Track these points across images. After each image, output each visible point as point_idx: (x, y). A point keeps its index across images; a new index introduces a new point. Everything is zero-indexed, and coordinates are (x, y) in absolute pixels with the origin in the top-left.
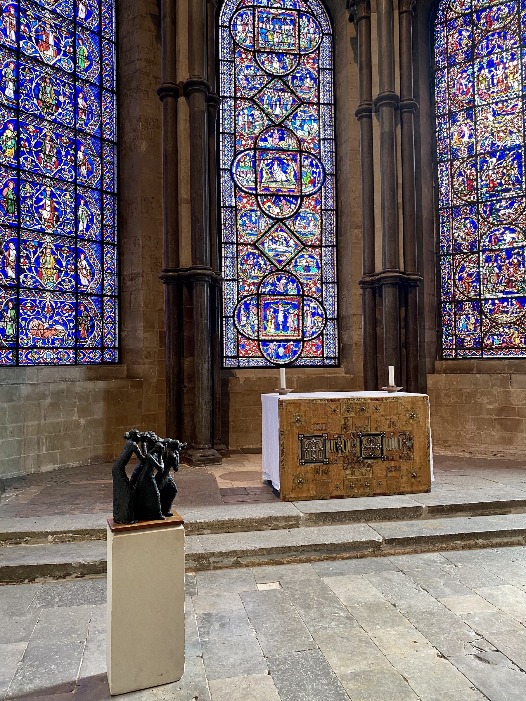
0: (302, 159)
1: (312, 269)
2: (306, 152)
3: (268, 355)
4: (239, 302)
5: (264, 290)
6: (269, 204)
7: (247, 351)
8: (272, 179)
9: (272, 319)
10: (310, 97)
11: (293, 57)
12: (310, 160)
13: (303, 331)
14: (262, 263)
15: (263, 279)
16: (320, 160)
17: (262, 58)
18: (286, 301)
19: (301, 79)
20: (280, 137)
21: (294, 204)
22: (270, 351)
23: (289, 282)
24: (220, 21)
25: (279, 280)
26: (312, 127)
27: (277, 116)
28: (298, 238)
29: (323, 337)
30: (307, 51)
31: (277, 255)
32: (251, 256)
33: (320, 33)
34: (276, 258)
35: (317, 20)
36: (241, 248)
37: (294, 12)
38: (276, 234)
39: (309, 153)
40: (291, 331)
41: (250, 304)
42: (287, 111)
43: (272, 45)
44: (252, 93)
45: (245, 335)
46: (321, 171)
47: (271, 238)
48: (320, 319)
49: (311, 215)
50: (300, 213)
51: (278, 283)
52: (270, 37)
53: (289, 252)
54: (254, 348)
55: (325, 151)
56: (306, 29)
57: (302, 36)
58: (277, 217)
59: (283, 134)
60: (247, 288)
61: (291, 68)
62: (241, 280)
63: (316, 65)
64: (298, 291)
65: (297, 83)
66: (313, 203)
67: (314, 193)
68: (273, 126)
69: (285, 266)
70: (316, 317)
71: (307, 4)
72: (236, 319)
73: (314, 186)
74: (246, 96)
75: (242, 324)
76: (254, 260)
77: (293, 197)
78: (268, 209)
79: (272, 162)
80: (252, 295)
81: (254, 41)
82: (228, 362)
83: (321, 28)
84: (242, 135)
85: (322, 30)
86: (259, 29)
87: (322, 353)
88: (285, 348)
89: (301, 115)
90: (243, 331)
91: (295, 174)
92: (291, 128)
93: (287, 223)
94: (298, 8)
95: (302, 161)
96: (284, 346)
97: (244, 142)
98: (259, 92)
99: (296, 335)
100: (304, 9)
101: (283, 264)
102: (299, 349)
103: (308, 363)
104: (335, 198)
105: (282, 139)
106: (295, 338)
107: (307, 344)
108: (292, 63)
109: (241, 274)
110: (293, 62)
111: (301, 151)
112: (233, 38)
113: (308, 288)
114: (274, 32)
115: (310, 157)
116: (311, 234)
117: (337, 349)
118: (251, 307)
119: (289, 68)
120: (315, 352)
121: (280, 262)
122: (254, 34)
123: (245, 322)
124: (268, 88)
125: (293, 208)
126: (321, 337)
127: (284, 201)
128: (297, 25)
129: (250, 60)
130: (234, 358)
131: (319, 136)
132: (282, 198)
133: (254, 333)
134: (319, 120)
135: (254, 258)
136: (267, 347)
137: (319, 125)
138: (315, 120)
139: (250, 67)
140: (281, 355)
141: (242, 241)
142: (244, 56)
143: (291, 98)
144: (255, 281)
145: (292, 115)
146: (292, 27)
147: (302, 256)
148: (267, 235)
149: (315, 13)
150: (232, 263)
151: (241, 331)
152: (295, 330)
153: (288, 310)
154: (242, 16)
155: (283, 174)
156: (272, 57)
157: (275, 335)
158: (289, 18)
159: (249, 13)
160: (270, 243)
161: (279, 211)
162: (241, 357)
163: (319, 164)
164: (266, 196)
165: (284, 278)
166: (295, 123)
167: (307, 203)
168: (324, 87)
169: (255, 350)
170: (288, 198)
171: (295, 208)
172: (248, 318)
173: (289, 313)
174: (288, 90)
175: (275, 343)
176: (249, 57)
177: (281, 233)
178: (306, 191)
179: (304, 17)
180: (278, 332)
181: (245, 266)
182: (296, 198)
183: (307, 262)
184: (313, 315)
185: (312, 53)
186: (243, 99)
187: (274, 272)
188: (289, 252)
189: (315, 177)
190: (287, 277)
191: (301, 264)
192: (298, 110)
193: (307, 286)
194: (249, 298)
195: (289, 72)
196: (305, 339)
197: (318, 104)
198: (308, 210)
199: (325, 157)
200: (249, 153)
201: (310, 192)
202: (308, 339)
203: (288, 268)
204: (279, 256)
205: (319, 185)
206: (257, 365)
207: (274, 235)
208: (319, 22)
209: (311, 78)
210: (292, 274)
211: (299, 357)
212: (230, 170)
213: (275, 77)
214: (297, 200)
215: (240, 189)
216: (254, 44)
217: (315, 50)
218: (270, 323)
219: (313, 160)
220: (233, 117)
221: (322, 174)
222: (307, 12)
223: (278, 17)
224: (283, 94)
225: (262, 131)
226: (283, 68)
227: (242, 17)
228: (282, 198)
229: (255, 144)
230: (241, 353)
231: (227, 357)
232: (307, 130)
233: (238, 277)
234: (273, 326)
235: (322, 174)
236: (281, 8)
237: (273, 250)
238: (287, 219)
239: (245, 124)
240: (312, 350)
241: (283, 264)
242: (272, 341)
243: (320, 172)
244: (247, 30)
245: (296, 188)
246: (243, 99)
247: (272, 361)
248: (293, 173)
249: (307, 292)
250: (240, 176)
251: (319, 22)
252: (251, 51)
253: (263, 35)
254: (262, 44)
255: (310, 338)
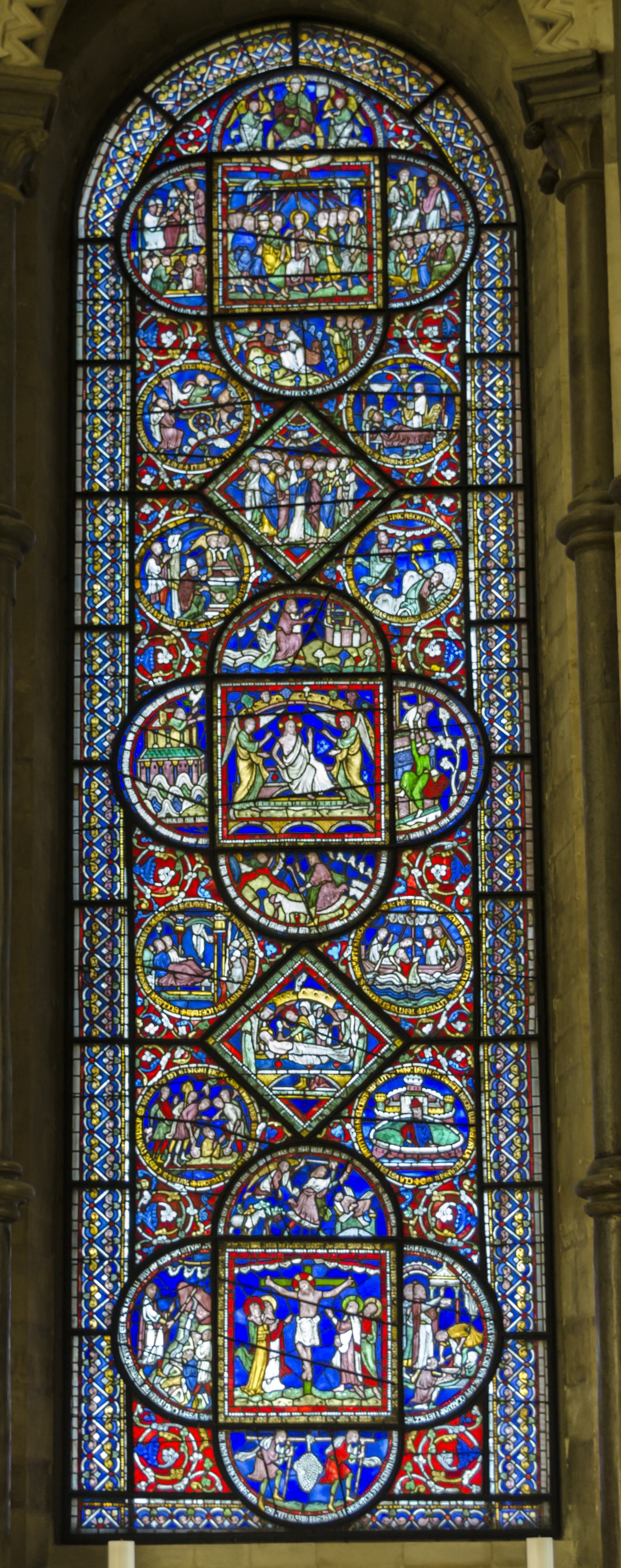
0: (396, 705)
1: (436, 1134)
2: (409, 675)
3: (254, 1486)
4: (135, 1271)
5: (237, 1220)
6: (260, 882)
7: (166, 1472)
8: (274, 789)
9: (270, 1337)
10: (428, 467)
11: (358, 324)
12: (429, 706)
13: (400, 1386)
14: (232, 1112)
15: (234, 1179)
16: (467, 703)
17: (241, 339)
18: (332, 1265)
19: (391, 401)
20: (305, 628)
21: (364, 878)
22: (259, 1472)
23: (339, 1189)
24: (82, 222)
25: (299, 1179)
26: (435, 579)
27: (295, 550)
28: (376, 1009)
29: (485, 1412)
30: (416, 296)
31: (294, 1080)
32: (187, 1088)
33: (467, 226)
34: (289, 1090)
35: (456, 178)
36: (147, 1057)
37: (364, 159)
38: (288, 998)
39: (425, 679)
40: (349, 1387)
41: (180, 1277)
42: (333, 525)
43: (277, 289)
44: (197, 473)
45: (160, 1402)
46: (474, 745)
47: (267, 1013)
48: (474, 1338)
49: (433, 919)
50: (389, 912)
51: (296, 1191)
52: (270, 258)
53: (342, 1067)
54: (197, 1456)
55: (489, 669)
56: (414, 215)
57: (395, 244)
58: (293, 930)
59: (319, 614)
60: (168, 1215)
61: (352, 366)
62: (145, 1183)
63: (451, 346)
64: (381, 1222)
65: (377, 417)
66: (440, 871)
67: (446, 833)
68: (279, 588)
69: (326, 1123)
70: (456, 1330)
71: (418, 126)
72: (123, 1340)
73: (446, 809)
74: (177, 484)
75: (149, 1359)
76: (197, 1101)
77: (360, 851)
78: (256, 904)
79: (272, 726)
80: (189, 1240)
81: (210, 280)
82: (91, 1516)
83: (474, 205)
84: (156, 630)
85: (477, 213)
86: (230, 236)
87: (483, 1478)
88: (323, 1459)
89: (392, 537)
90: (153, 1389)
91: (369, 765)
92: (350, 588)
93: (334, 952)
94: (381, 143)
95: (396, 712)
96: (319, 1450)
97: (164, 657)
98: (226, 464)
99: (371, 1402)
100: (403, 144)
101: (320, 1112)
102: (385, 1459)
103: (422, 1522)
104: (530, 846)
105: (312, 633)
106: (365, 1417)
107: (416, 1443)
108: (355, 346)
109: (145, 1160)
110: (362, 342)
111: (390, 674)
112: (127, 277)
113: (421, 1210)
114: (288, 240)
115: (430, 698)
116: (433, 993)
117: (545, 1462)
118: (183, 1292)
119: (343, 367)
120: (450, 1475)
121: (304, 1106)
122: (209, 254)
123: (160, 1351)
124: (261, 448)
125: (360, 895)
126: (475, 1410)
127: (321, 872)
128: (376, 203)
129: (194, 352)
130: (114, 1496)
131: (466, 611)
132: (313, 859)
133: (194, 1394)
134: (465, 550)
135: (201, 1096)
136: (250, 1455)
137: (466, 570)
138: (448, 554)
139: (196, 372)
140: (307, 1484)
141: (151, 1029)
142: (168, 338)
143: (351, 477)
144: (203, 1186)
145: (356, 542)
146: (358, 213)
147: (398, 1081)
148: (253, 1003)
149: (449, 153)
150: (113, 1119)
151: (145, 1389)
152: (368, 1381)
153: (338, 1299)
154: (165, 197)
155: (320, 766)
156: (280, 335)
157: (284, 1402)
158: (345, 183)
159: (191, 183)
160: (266, 1035)
161: (301, 908)
162: (142, 1495)
163: (463, 719)
164: (249, 853)
165: (322, 1172)
166: (368, 573)
167: (417, 873)
168: (484, 422)
169: (200, 1466)
170: (340, 856)
171: (367, 893)
172: (171, 1336)
173: (340, 1313)
174: (340, 448)
175: (281, 1437)
176: (190, 341)
177: (310, 993)
178: (412, 824)
179: (404, 176)
180: (297, 1392)
181: (162, 1128)
182: (369, 855)
183: (415, 1104)
184: (445, 1320)
185: (437, 300)
186: (164, 494)
187: (286, 1146)
188: (342, 1067)
189: (449, 772)
190: (334, 1165)
191: (391, 1113)
192: (379, 522)
193: (414, 1204)
194: (176, 1253)
195: (342, 380)
196: (409, 1420)
197: (461, 488)
198: (420, 901)
199: (489, 691)
200: (186, 696)
201: (430, 830)
202: (423, 1419)
203: (337, 1131)
204: (301, 1084)
205: (465, 799)
206: (208, 1525)
207: (280, 1001)
208: (462, 184)
209: (432, 397)
210: (352, 1152)
211: (386, 1493)
212: (112, 765)
213: (291, 403)
214: (372, 863)
215: (149, 831)
216: (211, 290)
217: (449, 290)
218: (261, 1353)
219: (438, 703)
220: (125, 567)
221: (475, 758)
222: (417, 153)
223: (303, 182)
224: (319, 466)
225: (237, 611)
226: (320, 368)
227: (165, 198)
228: (313, 859)
229: (210, 658)
230: (145, 1479)
231: (89, 1496)
232: (413, 595)
233: (133, 1172)
234: (274, 1368)
235: (475, 758)
236: (315, 151)
237: (279, 1063)
238: (334, 936)
239: (168, 590)
240: (439, 1467)
241: (320, 1112)
242: (269, 1430)
243: (466, 752)
244: (181, 243)
245: (370, 817)
246: (164, 494)
247: (271, 1511)
248: (357, 761)
249: (417, 1227)
250: (148, 785)
251: (462, 184)
252: (198, 317)
253: (245, 256)
254: (239, 289)
255: (432, 1416)
